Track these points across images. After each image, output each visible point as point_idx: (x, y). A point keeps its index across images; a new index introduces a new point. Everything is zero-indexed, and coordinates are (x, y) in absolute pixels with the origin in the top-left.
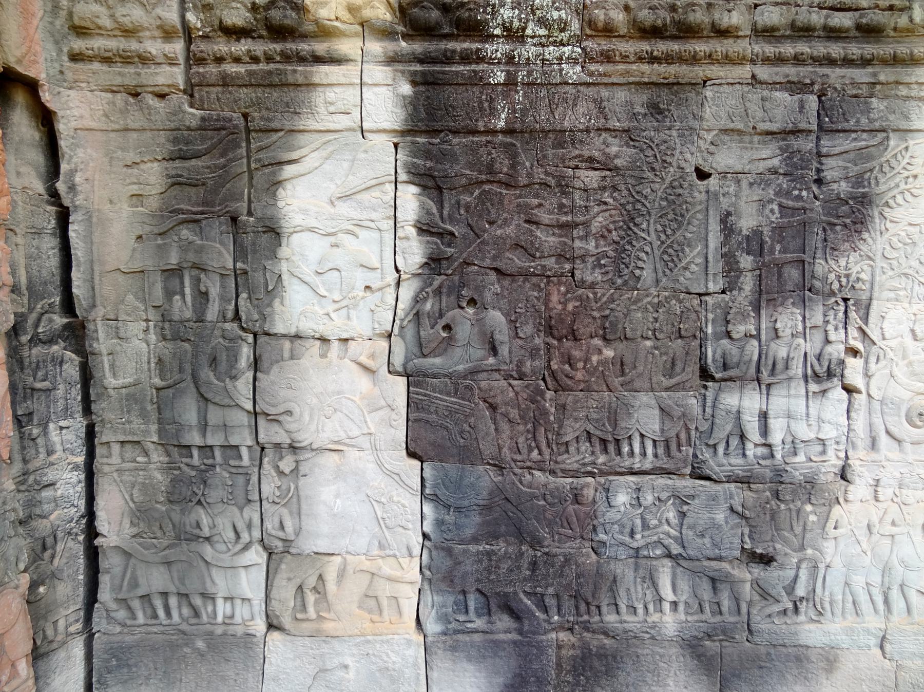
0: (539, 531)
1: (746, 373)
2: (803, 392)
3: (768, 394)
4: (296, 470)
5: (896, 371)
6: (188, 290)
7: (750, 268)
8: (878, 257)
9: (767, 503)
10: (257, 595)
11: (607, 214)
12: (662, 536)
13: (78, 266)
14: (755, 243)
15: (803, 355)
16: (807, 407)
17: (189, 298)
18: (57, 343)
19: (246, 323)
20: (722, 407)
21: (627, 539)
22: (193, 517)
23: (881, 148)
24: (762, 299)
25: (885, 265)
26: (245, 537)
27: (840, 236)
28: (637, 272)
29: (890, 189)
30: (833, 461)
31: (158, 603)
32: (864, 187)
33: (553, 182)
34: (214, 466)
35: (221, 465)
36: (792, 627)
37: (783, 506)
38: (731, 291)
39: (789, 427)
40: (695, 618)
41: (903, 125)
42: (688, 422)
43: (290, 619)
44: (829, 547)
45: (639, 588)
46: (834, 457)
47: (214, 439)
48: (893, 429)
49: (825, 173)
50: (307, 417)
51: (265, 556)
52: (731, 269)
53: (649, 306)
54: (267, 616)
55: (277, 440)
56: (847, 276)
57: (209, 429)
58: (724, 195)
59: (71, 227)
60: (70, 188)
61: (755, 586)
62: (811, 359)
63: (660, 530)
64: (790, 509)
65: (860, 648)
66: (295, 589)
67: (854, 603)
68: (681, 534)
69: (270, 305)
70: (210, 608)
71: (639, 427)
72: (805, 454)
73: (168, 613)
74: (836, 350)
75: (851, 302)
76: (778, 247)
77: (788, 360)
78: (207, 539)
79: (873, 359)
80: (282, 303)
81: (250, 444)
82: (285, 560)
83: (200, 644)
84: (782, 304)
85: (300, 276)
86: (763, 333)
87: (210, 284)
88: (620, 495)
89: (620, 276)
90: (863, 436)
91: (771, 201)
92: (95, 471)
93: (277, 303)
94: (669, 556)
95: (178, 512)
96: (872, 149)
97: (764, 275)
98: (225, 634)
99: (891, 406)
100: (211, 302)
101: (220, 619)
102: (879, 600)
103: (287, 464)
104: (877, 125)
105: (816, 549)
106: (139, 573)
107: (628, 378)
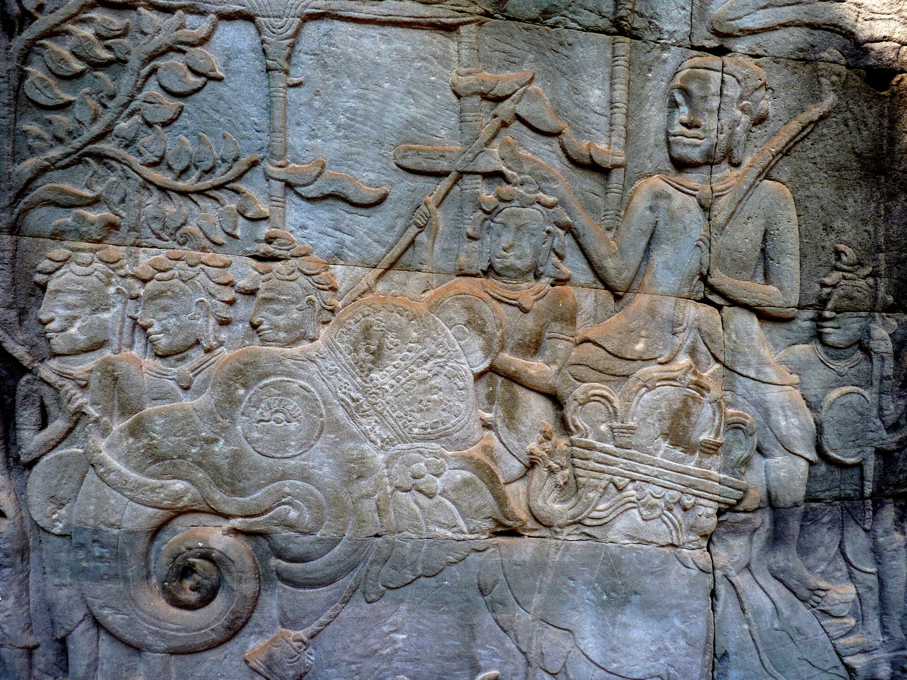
48: (109, 616)
90: (30, 641)
99: (97, 551)
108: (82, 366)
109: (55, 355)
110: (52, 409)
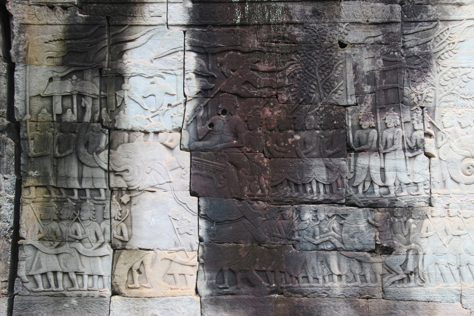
0: (262, 234)
1: (371, 147)
2: (403, 157)
3: (384, 159)
4: (129, 202)
5: (453, 144)
6: (75, 106)
7: (370, 92)
8: (437, 85)
9: (387, 218)
10: (107, 272)
11: (294, 66)
12: (330, 237)
13: (18, 93)
14: (371, 79)
15: (401, 137)
16: (406, 165)
17: (75, 110)
18: (5, 134)
19: (105, 123)
20: (359, 165)
21: (311, 239)
22: (72, 229)
23: (435, 30)
24: (379, 108)
25: (441, 89)
26: (102, 239)
27: (416, 75)
28: (311, 95)
29: (441, 50)
30: (423, 193)
31: (51, 277)
32: (427, 49)
33: (265, 49)
34: (86, 200)
35: (89, 199)
36: (407, 289)
37: (397, 220)
38: (360, 104)
39: (397, 176)
40: (352, 284)
41: (446, 17)
42: (342, 174)
43: (125, 288)
44: (424, 243)
45: (320, 268)
46: (424, 193)
47: (86, 185)
48: (454, 177)
49: (406, 43)
50: (136, 173)
51: (112, 251)
52: (359, 93)
53: (317, 113)
54: (112, 286)
55: (120, 186)
56: (421, 95)
57: (84, 179)
58: (354, 55)
59: (15, 73)
60: (16, 53)
61: (384, 265)
62: (407, 139)
63: (329, 233)
64: (400, 221)
65: (448, 302)
66: (128, 270)
67: (441, 274)
68: (342, 236)
69: (118, 114)
70: (80, 281)
71: (315, 177)
72: (408, 191)
73: (57, 286)
74: (419, 134)
75: (424, 109)
76: (384, 81)
77: (393, 140)
78: (80, 241)
79: (439, 139)
80: (124, 113)
81: (105, 187)
82: (123, 253)
83: (74, 301)
84: (388, 110)
85: (134, 99)
86: (379, 126)
87: (87, 103)
88: (306, 214)
89: (302, 97)
90: (439, 181)
91: (378, 58)
92: (21, 202)
93: (122, 112)
94: (335, 249)
95: (65, 225)
96: (431, 30)
97: (377, 95)
98: (87, 296)
99: (452, 163)
100: (87, 112)
101: (85, 288)
102: (456, 273)
103: (125, 199)
104: (432, 18)
105: (417, 244)
106: (42, 259)
107: (307, 151)
108: (449, 130)
109: (445, 128)
110: (444, 137)
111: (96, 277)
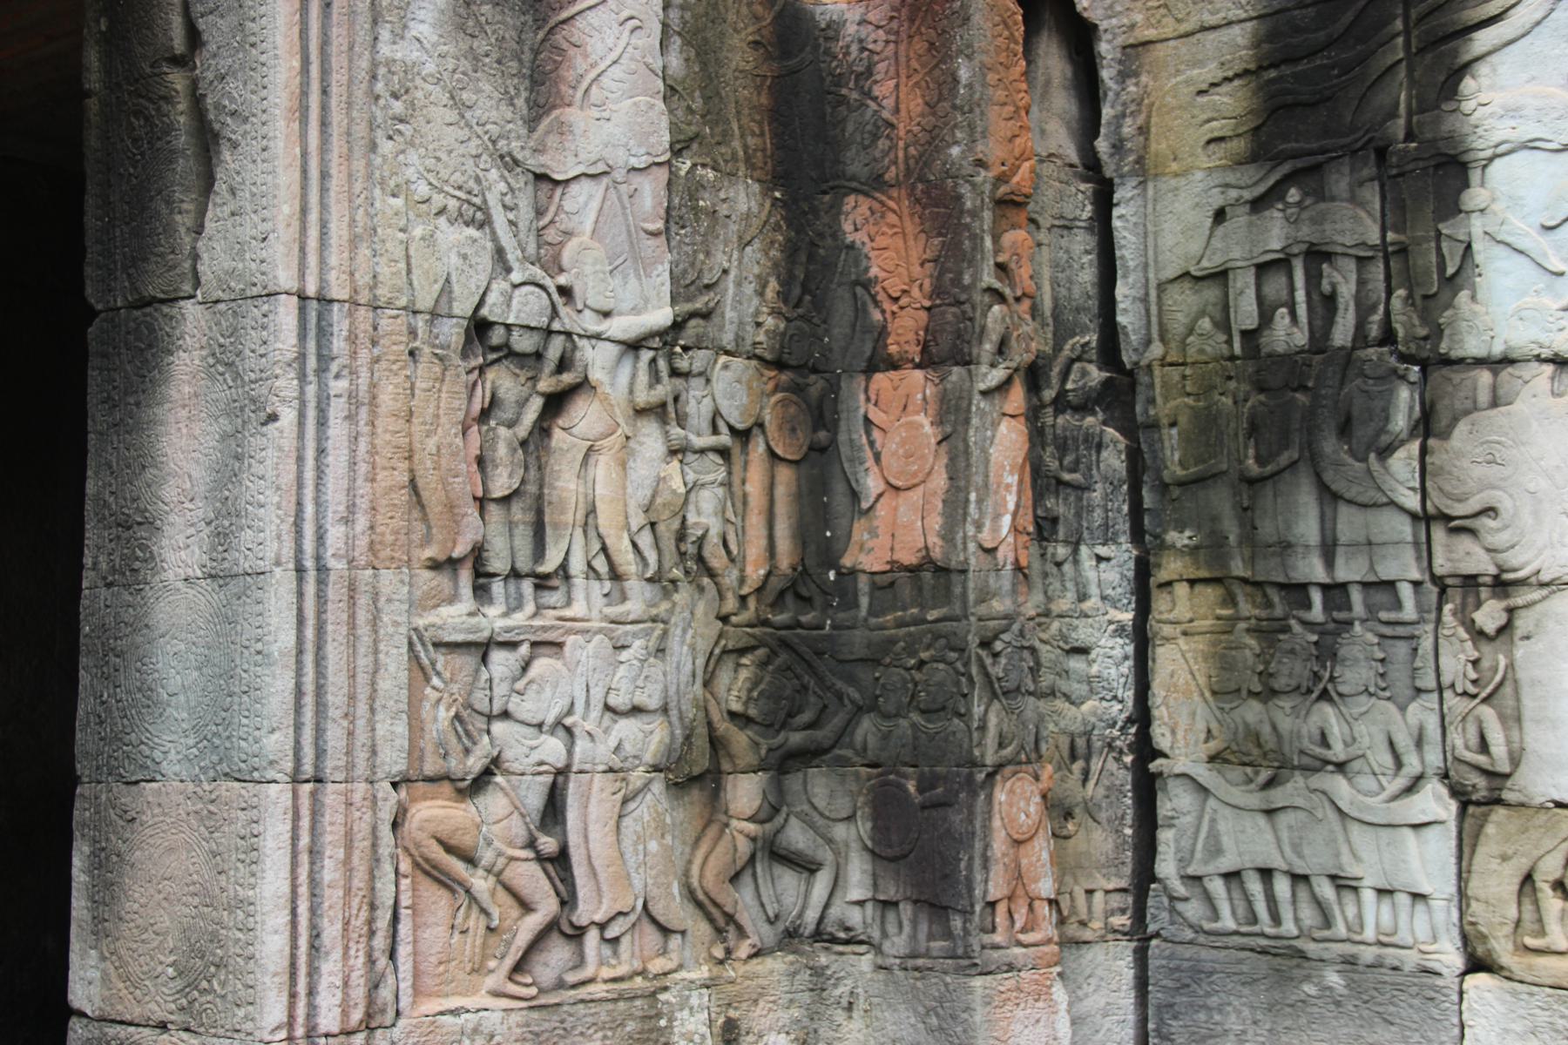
4: (1505, 629)
6: (1300, 295)
13: (1125, 276)
17: (1302, 310)
18: (1094, 413)
19: (1406, 343)
22: (1314, 722)
26: (1413, 764)
31: (1255, 886)
34: (1350, 623)
35: (1363, 621)
43: (1510, 947)
47: (1347, 570)
50: (1527, 519)
51: (1453, 806)
54: (1465, 938)
55: (1469, 568)
57: (1340, 551)
59: (1116, 212)
60: (1114, 146)
66: (1517, 881)
69: (1449, 305)
70: (1351, 911)
73: (1276, 919)
78: (1341, 767)
80: (1473, 298)
81: (1416, 576)
82: (1494, 817)
83: (1334, 979)
85: (1509, 239)
87: (1338, 278)
92: (1150, 635)
93: (1463, 296)
95: (1288, 711)
98: (1377, 965)
100: (1341, 312)
101: (1369, 934)
103: (1489, 615)
106: (1222, 826)
111: (1403, 900)
